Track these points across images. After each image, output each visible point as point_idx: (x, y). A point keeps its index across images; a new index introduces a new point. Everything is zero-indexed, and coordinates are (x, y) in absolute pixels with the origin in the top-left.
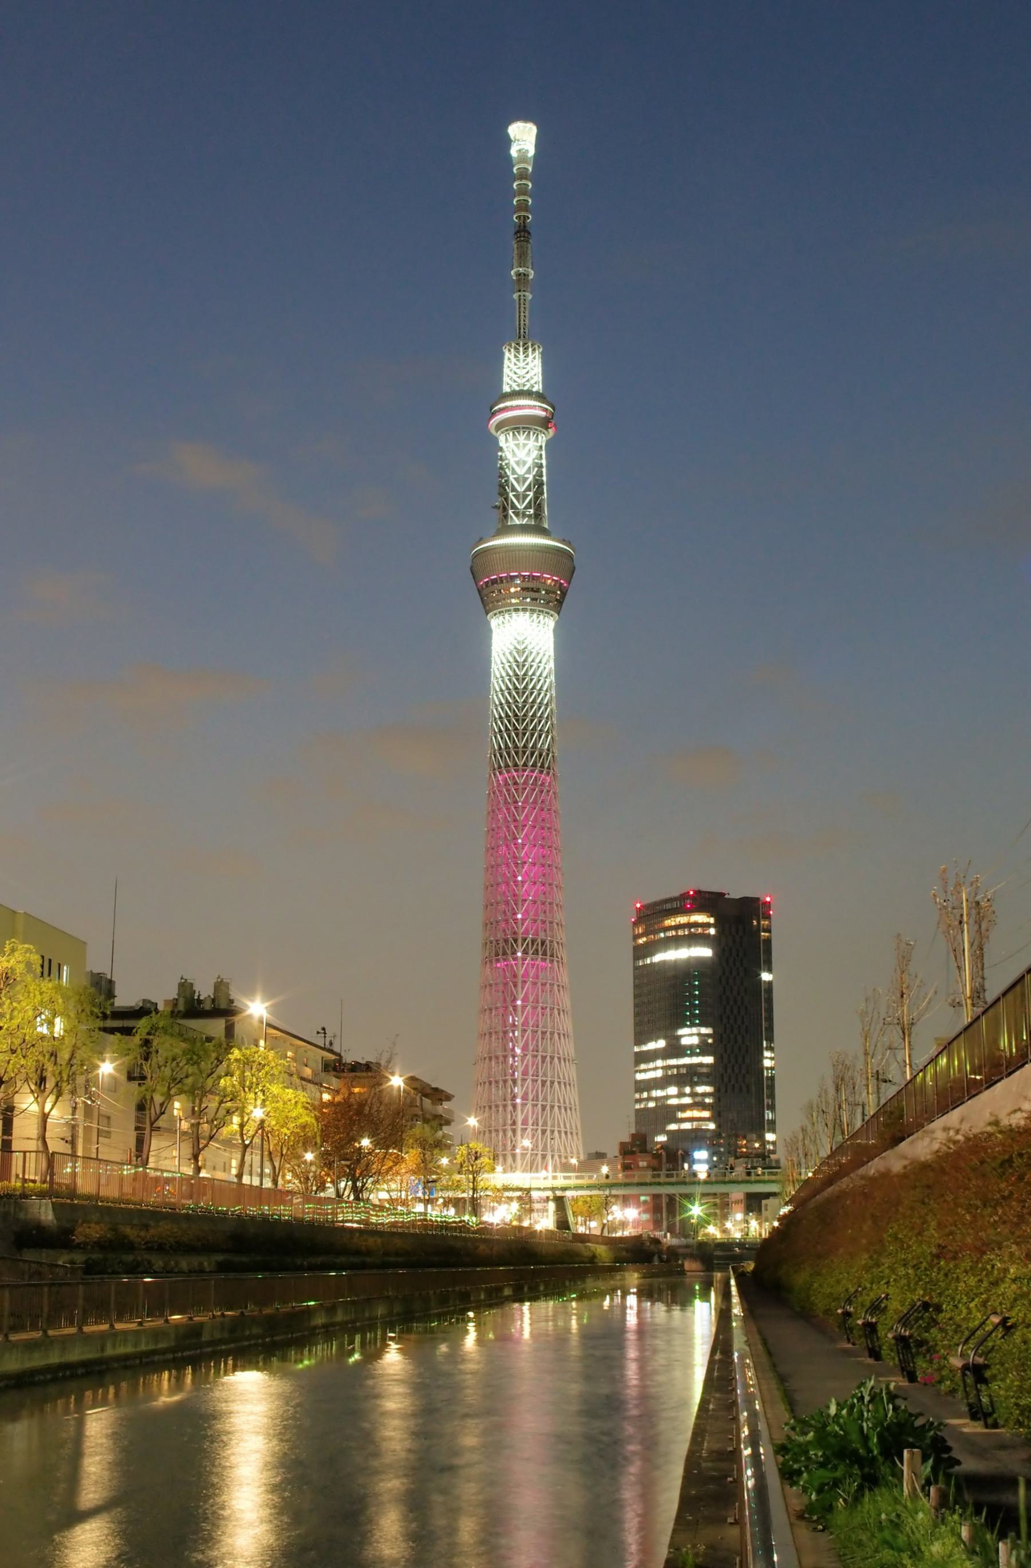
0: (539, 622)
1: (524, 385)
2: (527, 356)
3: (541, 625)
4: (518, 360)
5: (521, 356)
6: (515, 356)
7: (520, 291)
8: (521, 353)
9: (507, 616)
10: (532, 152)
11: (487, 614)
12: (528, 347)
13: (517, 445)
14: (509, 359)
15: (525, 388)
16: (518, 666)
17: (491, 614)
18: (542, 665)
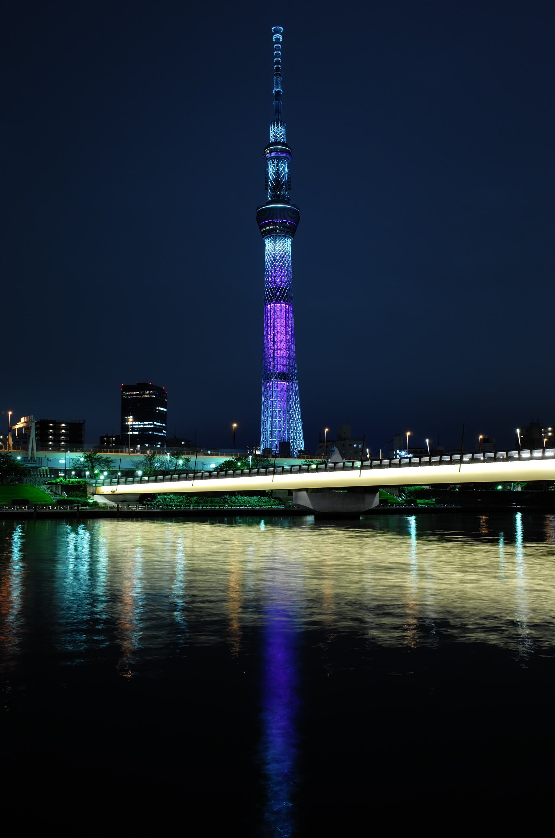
0: (283, 240)
1: (277, 140)
2: (278, 127)
3: (284, 242)
4: (275, 129)
5: (276, 128)
6: (274, 128)
7: (276, 100)
8: (276, 126)
9: (269, 239)
10: (281, 41)
11: (263, 237)
12: (279, 124)
13: (274, 166)
14: (271, 129)
15: (278, 141)
16: (273, 260)
17: (264, 238)
18: (284, 259)
